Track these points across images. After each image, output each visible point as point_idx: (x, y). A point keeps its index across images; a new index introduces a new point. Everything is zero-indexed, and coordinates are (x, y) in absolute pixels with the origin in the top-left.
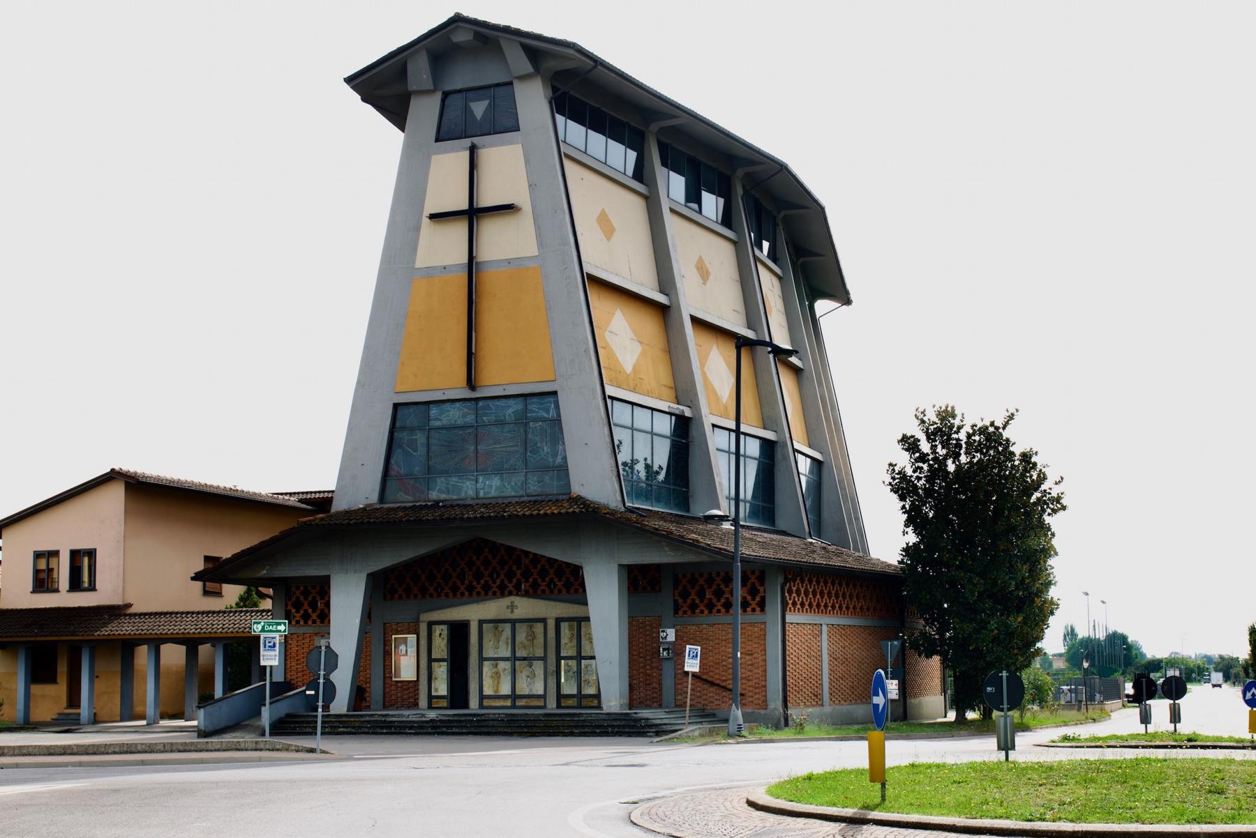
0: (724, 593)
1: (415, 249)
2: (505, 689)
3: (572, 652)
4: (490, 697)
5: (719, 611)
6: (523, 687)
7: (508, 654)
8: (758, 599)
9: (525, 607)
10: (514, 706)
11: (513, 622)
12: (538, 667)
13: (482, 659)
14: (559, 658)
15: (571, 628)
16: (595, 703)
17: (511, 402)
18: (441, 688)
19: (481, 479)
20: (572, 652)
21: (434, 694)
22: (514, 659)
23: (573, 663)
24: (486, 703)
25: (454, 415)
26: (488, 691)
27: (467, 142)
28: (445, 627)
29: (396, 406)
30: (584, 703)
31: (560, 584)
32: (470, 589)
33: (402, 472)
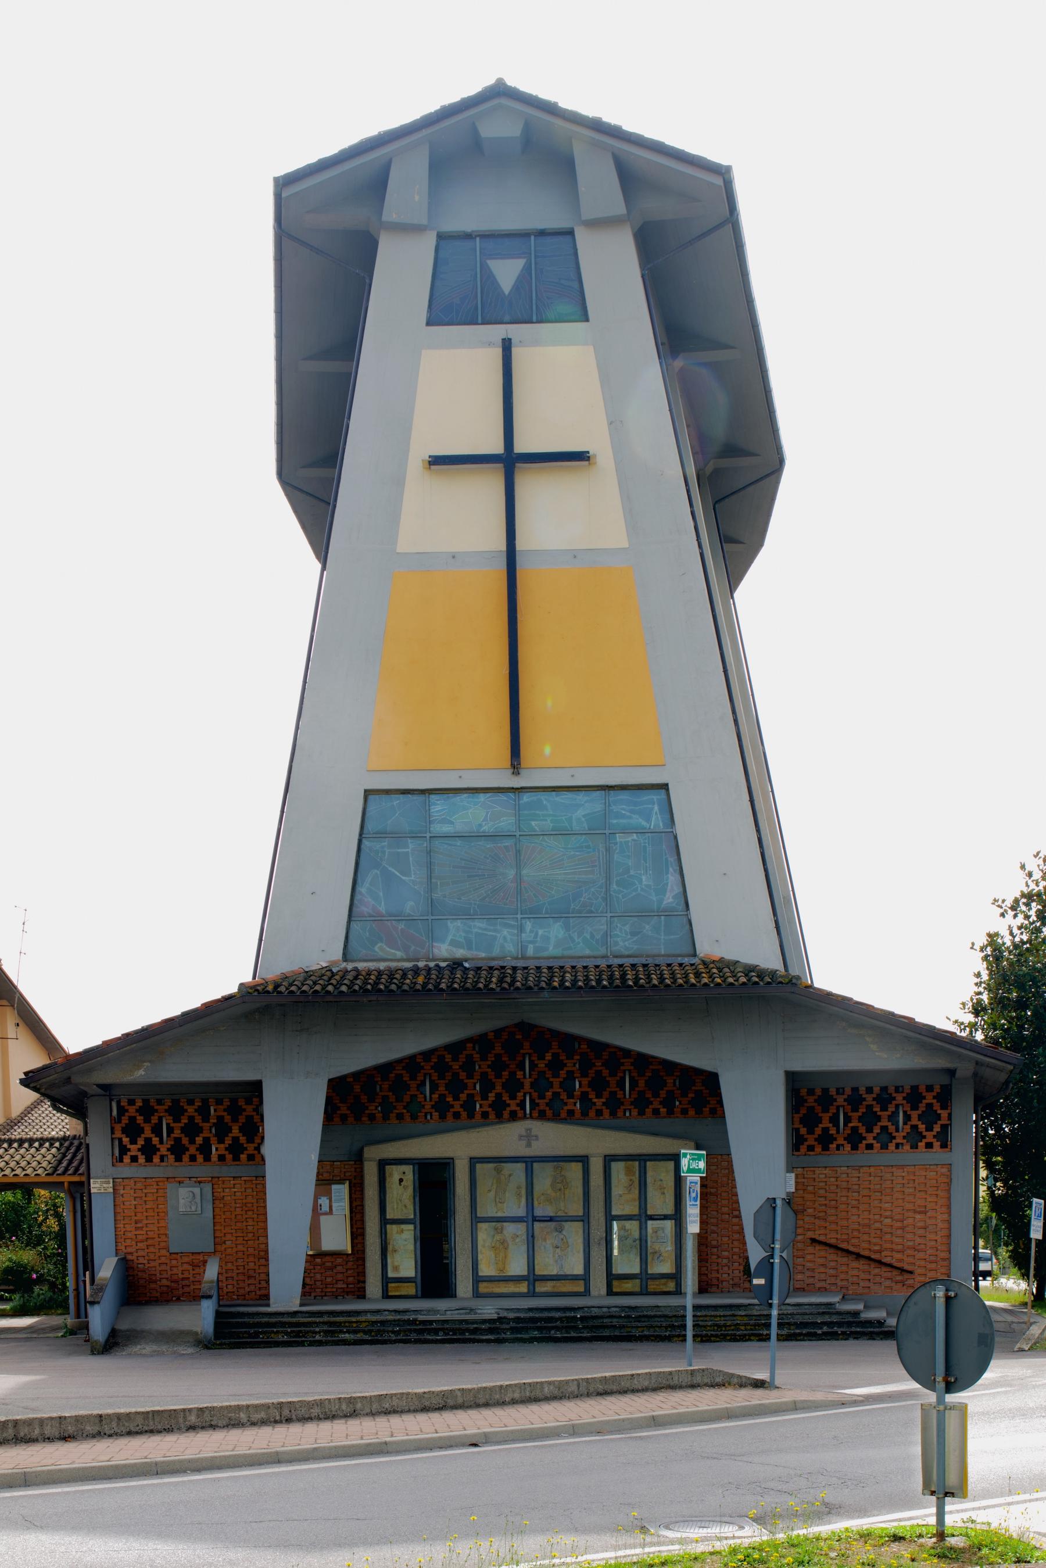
0: (879, 1118)
1: (395, 518)
2: (517, 1266)
3: (633, 1209)
4: (490, 1280)
5: (870, 1147)
6: (547, 1264)
7: (521, 1212)
8: (937, 1128)
9: (553, 1137)
10: (532, 1294)
11: (529, 1162)
12: (574, 1233)
13: (476, 1220)
14: (610, 1218)
15: (629, 1171)
16: (671, 1286)
17: (581, 797)
18: (405, 1263)
19: (528, 925)
20: (633, 1209)
21: (391, 1274)
22: (532, 1219)
23: (633, 1226)
24: (483, 1288)
25: (473, 815)
26: (486, 1269)
27: (499, 331)
28: (408, 1169)
29: (368, 793)
30: (652, 1286)
31: (599, 1102)
32: (442, 1109)
33: (382, 908)
